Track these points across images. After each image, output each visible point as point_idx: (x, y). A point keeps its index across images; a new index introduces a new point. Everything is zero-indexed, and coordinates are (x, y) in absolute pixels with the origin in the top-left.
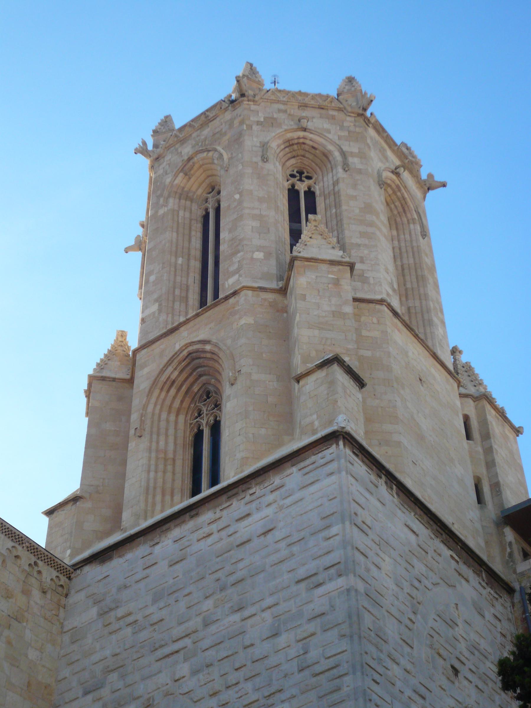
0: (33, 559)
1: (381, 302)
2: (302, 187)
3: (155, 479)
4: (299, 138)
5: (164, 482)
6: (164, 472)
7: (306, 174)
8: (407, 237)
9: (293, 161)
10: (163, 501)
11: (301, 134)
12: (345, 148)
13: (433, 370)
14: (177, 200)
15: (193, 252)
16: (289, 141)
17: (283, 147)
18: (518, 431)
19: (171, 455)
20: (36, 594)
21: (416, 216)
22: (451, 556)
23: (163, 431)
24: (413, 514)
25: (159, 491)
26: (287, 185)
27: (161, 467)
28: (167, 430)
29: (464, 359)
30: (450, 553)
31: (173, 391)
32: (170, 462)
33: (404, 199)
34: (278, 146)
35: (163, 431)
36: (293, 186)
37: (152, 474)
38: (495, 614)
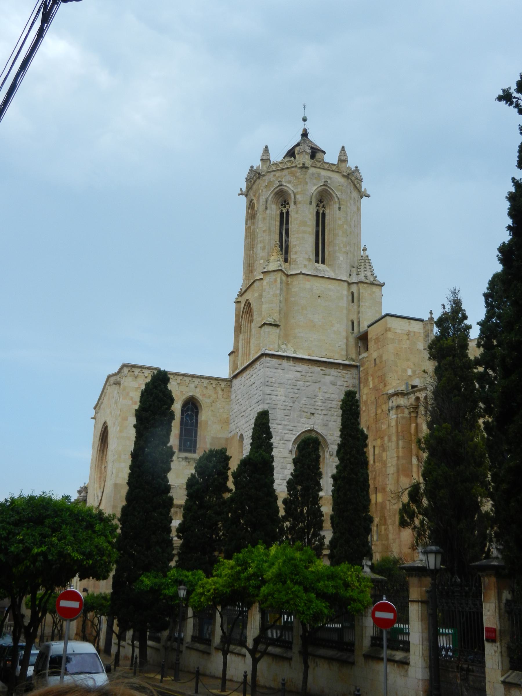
0: (217, 382)
1: (301, 273)
2: (284, 211)
3: (244, 350)
4: (280, 189)
5: (247, 351)
6: (247, 347)
7: (287, 202)
8: (333, 212)
9: (281, 198)
10: (246, 359)
11: (280, 188)
12: (295, 191)
13: (330, 287)
14: (250, 221)
15: (277, 219)
16: (276, 193)
17: (274, 196)
18: (382, 285)
19: (248, 340)
20: (220, 392)
21: (336, 200)
22: (322, 370)
23: (246, 331)
24: (300, 364)
25: (245, 355)
26: (278, 212)
27: (246, 345)
28: (248, 330)
29: (367, 253)
30: (321, 368)
31: (248, 315)
32: (248, 343)
33: (331, 193)
34: (272, 198)
35: (246, 331)
36: (282, 210)
37: (243, 349)
38: (274, 427)
